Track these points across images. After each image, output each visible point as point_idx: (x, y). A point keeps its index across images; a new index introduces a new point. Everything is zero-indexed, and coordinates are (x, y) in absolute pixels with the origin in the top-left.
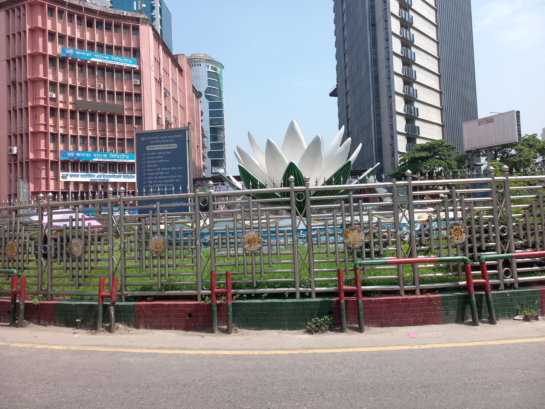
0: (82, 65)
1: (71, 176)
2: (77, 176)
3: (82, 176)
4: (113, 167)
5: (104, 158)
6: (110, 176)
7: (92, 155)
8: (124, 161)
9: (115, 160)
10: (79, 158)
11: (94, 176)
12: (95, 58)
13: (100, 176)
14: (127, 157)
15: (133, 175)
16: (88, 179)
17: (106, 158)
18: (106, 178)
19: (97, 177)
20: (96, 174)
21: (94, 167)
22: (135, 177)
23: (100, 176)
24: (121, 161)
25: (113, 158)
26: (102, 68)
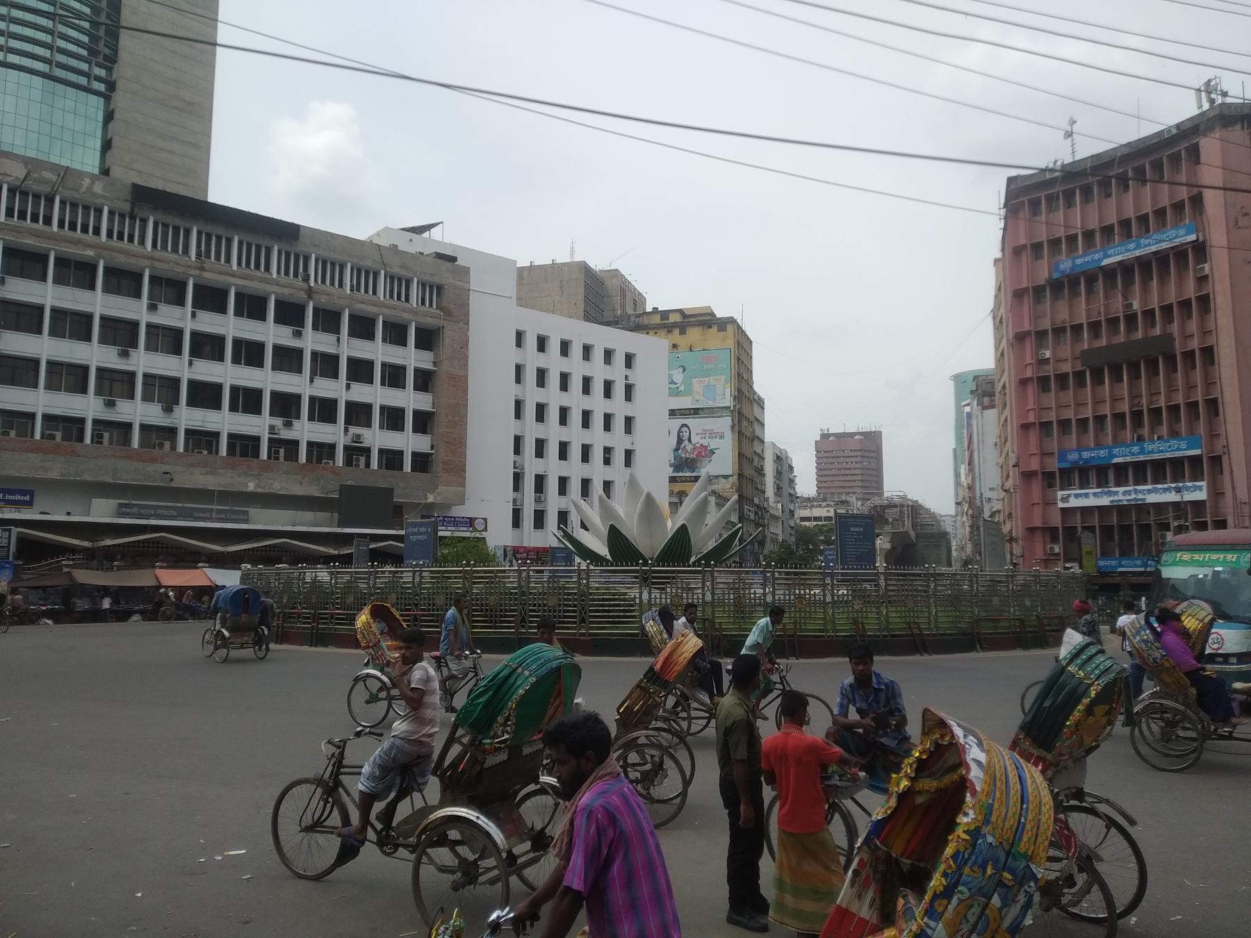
0: (1091, 278)
1: (1077, 496)
2: (1087, 495)
3: (1095, 494)
4: (1159, 470)
5: (1133, 454)
6: (1149, 491)
7: (1110, 452)
8: (1177, 454)
9: (1156, 456)
10: (1087, 461)
11: (1116, 493)
12: (1110, 256)
13: (1129, 493)
14: (1184, 445)
16: (1105, 501)
18: (1140, 496)
19: (1122, 494)
20: (1121, 489)
21: (1122, 474)
22: (1205, 489)
23: (1129, 493)
24: (1168, 455)
25: (1152, 452)
26: (1126, 268)
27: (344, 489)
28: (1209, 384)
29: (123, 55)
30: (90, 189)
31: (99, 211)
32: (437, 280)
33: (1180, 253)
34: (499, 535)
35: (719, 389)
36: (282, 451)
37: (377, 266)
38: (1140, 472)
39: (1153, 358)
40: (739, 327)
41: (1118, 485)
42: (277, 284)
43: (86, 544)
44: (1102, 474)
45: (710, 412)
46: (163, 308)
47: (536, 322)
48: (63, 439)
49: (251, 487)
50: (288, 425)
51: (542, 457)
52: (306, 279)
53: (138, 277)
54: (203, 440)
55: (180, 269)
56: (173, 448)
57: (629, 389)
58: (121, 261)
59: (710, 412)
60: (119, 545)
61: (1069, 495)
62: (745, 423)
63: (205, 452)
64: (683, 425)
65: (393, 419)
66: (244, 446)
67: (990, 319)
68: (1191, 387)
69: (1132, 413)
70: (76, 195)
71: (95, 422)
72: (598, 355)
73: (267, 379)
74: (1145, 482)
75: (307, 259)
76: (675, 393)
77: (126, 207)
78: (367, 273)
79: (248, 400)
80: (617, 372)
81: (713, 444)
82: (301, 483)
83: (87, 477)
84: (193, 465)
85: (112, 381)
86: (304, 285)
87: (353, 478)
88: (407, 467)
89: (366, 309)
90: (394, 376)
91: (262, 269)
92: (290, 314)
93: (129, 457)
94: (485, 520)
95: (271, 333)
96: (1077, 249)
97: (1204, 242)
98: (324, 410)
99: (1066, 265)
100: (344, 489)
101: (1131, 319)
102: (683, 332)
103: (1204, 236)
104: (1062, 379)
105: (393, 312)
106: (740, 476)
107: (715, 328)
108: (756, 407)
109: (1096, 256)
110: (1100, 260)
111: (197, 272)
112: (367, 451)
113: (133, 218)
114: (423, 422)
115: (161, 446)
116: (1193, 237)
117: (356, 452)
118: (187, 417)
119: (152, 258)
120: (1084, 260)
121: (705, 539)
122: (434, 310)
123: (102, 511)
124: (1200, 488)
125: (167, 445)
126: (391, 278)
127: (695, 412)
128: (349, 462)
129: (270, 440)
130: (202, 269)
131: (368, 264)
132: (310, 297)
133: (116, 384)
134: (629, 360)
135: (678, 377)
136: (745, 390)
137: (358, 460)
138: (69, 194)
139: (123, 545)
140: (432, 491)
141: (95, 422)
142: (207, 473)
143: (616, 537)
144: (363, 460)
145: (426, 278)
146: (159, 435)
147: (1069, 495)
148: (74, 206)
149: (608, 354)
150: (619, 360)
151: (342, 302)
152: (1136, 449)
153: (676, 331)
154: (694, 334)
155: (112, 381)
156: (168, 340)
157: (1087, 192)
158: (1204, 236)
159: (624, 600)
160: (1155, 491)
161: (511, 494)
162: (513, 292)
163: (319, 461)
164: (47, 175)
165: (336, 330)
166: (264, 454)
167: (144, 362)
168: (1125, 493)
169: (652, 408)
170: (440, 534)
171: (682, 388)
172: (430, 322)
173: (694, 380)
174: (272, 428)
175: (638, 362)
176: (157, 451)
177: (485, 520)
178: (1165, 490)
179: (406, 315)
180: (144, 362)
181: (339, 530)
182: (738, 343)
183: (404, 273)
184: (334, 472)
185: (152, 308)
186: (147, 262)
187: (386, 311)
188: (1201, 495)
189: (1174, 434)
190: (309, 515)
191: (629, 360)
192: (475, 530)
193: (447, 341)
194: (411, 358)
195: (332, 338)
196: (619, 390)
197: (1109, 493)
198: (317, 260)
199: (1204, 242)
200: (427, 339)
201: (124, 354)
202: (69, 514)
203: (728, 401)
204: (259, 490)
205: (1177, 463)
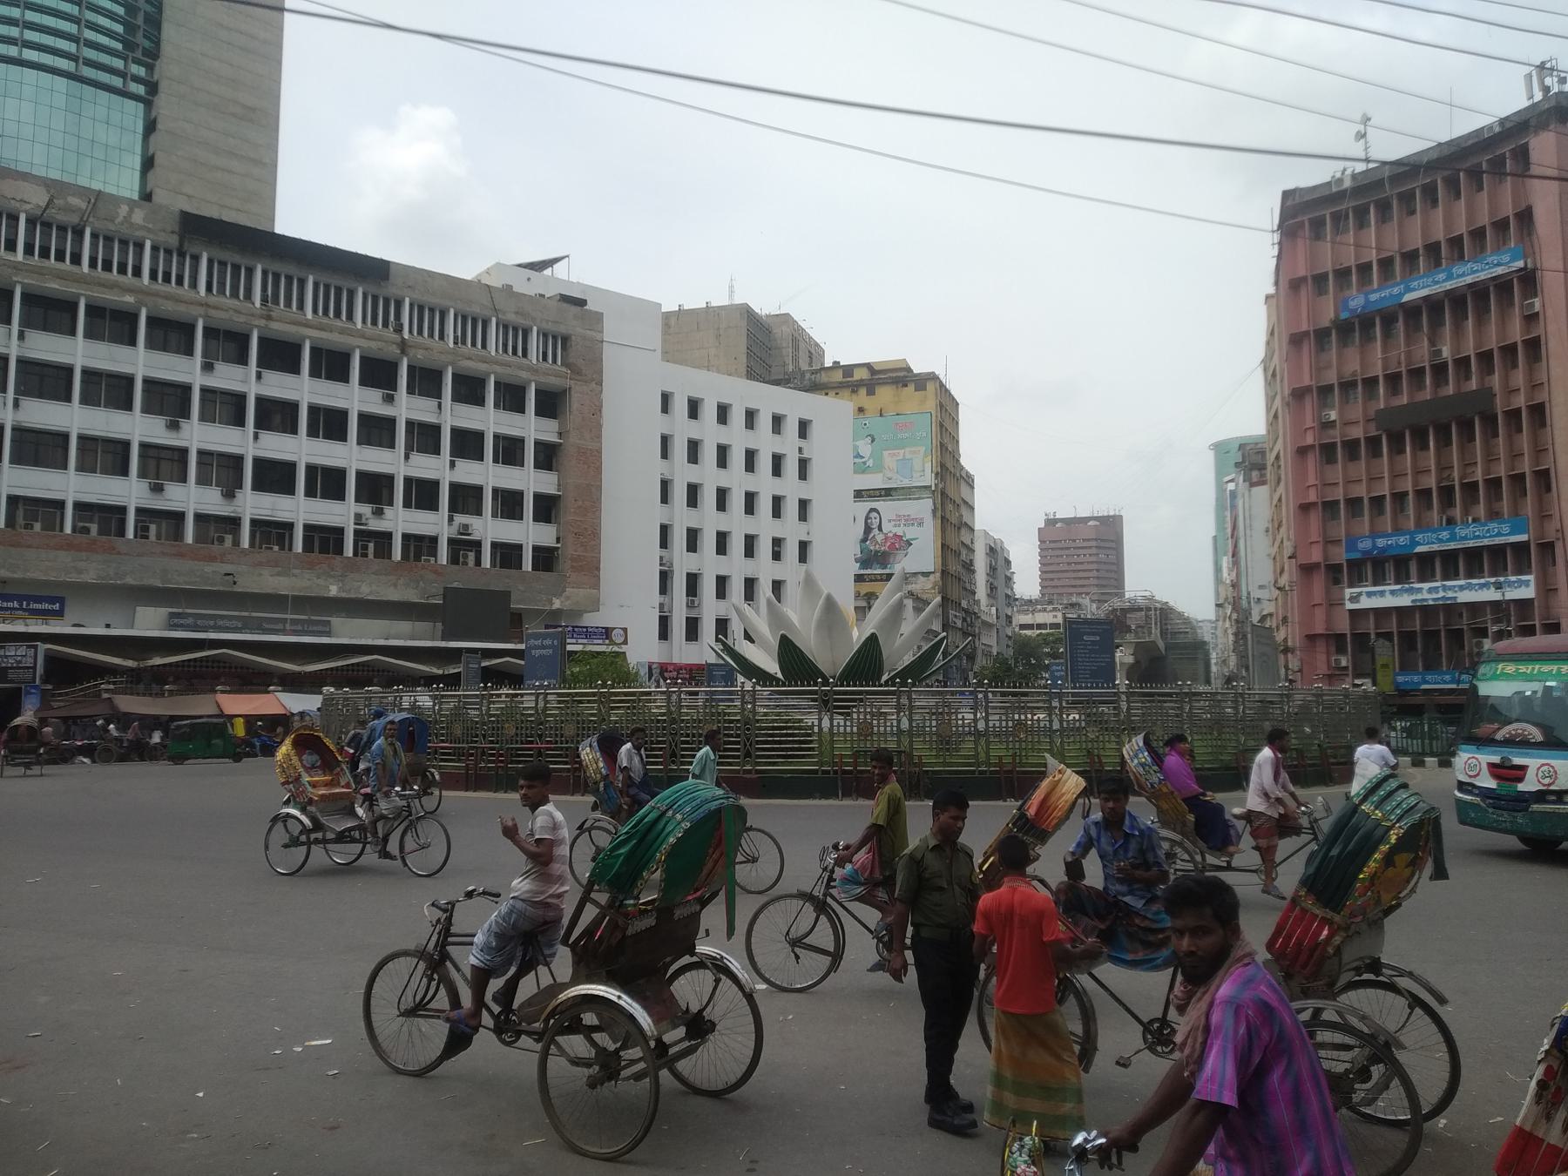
0: (1388, 319)
1: (1369, 594)
2: (1382, 593)
3: (1393, 592)
4: (1474, 561)
5: (1441, 541)
6: (1462, 588)
9: (1471, 544)
10: (1383, 550)
11: (1420, 590)
15: (1524, 578)
16: (1405, 601)
17: (1449, 540)
18: (1450, 594)
19: (1428, 592)
20: (1426, 586)
21: (1427, 566)
22: (1532, 584)
24: (1486, 542)
25: (1465, 538)
26: (1433, 305)
27: (448, 593)
28: (1539, 451)
29: (166, 49)
30: (127, 219)
31: (140, 246)
32: (562, 329)
33: (1503, 286)
34: (643, 650)
35: (917, 464)
36: (371, 545)
37: (487, 313)
38: (1450, 563)
39: (1468, 419)
40: (942, 386)
41: (1422, 579)
42: (363, 336)
43: (130, 663)
44: (1400, 567)
45: (906, 493)
46: (221, 367)
47: (687, 381)
48: (101, 533)
49: (334, 591)
50: (379, 513)
51: (695, 551)
52: (399, 329)
53: (190, 329)
54: (272, 532)
55: (242, 319)
56: (236, 543)
57: (803, 465)
58: (168, 309)
59: (906, 493)
60: (170, 664)
61: (1360, 594)
62: (950, 507)
63: (276, 548)
64: (872, 510)
65: (509, 504)
66: (324, 539)
67: (1260, 372)
68: (1515, 456)
69: (1440, 489)
70: (113, 228)
71: (139, 511)
72: (764, 422)
73: (351, 456)
74: (1456, 576)
75: (399, 304)
76: (861, 469)
77: (173, 241)
78: (475, 321)
79: (328, 482)
80: (788, 444)
81: (910, 532)
82: (395, 585)
83: (129, 580)
84: (260, 564)
85: (159, 459)
86: (396, 337)
87: (461, 579)
88: (527, 564)
89: (472, 366)
90: (510, 451)
91: (344, 317)
92: (379, 374)
93: (181, 555)
94: (625, 630)
95: (355, 398)
96: (1371, 281)
97: (1534, 270)
98: (423, 494)
99: (1357, 301)
100: (448, 593)
101: (1440, 370)
102: (871, 392)
103: (1534, 262)
104: (1351, 447)
105: (509, 371)
106: (944, 573)
107: (911, 387)
108: (963, 485)
109: (1396, 290)
110: (1401, 295)
111: (263, 322)
112: (477, 545)
113: (182, 255)
114: (546, 508)
115: (221, 540)
116: (1520, 264)
117: (463, 546)
118: (253, 504)
119: (207, 305)
120: (1380, 295)
121: (900, 652)
122: (559, 367)
123: (149, 623)
124: (1527, 583)
125: (229, 539)
126: (504, 327)
127: (887, 493)
128: (454, 559)
129: (356, 531)
130: (269, 318)
131: (476, 310)
132: (403, 352)
133: (164, 463)
134: (804, 428)
135: (865, 448)
136: (949, 465)
137: (466, 557)
138: (99, 225)
139: (177, 664)
140: (558, 595)
141: (139, 511)
142: (279, 574)
143: (788, 651)
144: (471, 556)
145: (550, 327)
146: (219, 527)
147: (1360, 594)
148: (109, 240)
149: (777, 421)
150: (791, 427)
151: (443, 357)
152: (1445, 534)
153: (863, 391)
154: (885, 394)
155: (159, 459)
156: (228, 407)
157: (1384, 208)
158: (1534, 262)
159: (800, 728)
160: (1469, 587)
161: (656, 598)
162: (657, 343)
163: (417, 558)
164: (74, 201)
165: (437, 394)
166: (349, 550)
167: (198, 435)
168: (1430, 590)
169: (833, 489)
170: (569, 648)
171: (870, 463)
172: (553, 382)
173: (886, 453)
174: (358, 516)
175: (815, 431)
176: (216, 547)
177: (625, 630)
178: (1482, 586)
179: (524, 375)
180: (198, 435)
181: (443, 644)
182: (941, 406)
183: (520, 321)
184: (435, 572)
185: (208, 367)
186: (201, 310)
187: (498, 369)
188: (1528, 592)
189: (1494, 515)
190: (404, 626)
191: (804, 428)
192: (613, 643)
193: (575, 405)
194: (531, 427)
195: (431, 403)
196: (790, 467)
197: (1411, 591)
198: (411, 305)
199: (1534, 270)
200: (550, 404)
201: (174, 426)
202: (108, 626)
203: (928, 479)
204: (344, 595)
205: (1498, 552)
